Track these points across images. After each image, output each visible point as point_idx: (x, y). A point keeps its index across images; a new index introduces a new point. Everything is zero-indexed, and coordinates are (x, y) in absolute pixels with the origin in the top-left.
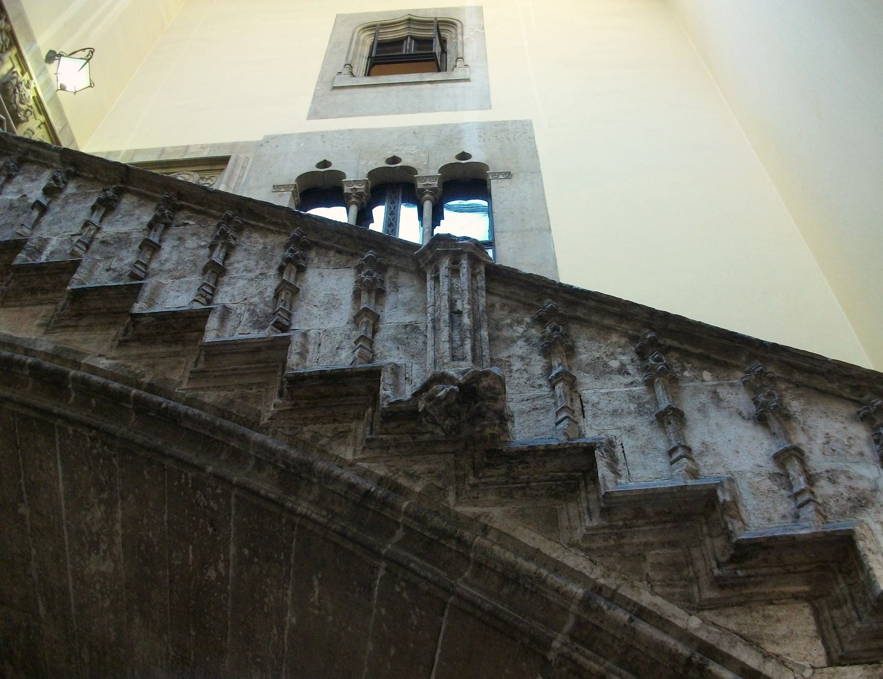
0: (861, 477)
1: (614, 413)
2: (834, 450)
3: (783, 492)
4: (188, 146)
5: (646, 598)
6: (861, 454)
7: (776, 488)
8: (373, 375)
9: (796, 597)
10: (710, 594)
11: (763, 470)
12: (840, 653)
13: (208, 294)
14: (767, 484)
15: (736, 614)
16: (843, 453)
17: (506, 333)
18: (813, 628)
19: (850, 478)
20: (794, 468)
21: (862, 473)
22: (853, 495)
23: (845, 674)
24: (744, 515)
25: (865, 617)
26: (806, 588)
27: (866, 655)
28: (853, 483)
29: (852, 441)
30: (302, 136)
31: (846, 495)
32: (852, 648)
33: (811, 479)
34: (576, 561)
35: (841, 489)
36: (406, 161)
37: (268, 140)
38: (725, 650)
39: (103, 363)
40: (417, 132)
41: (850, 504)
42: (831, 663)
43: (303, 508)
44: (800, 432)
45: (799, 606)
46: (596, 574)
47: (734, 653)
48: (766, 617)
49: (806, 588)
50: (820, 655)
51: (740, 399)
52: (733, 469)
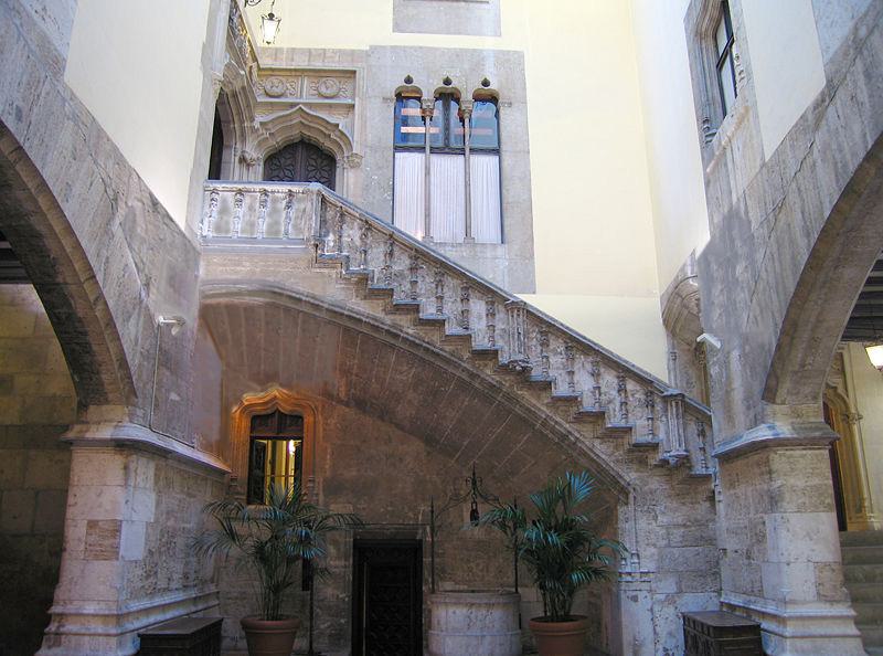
1: (558, 368)
4: (325, 50)
5: (558, 419)
8: (496, 352)
13: (440, 310)
17: (531, 335)
30: (394, 48)
34: (544, 409)
36: (455, 84)
37: (374, 49)
39: (410, 331)
40: (459, 54)
43: (477, 385)
46: (548, 412)
51: (589, 367)
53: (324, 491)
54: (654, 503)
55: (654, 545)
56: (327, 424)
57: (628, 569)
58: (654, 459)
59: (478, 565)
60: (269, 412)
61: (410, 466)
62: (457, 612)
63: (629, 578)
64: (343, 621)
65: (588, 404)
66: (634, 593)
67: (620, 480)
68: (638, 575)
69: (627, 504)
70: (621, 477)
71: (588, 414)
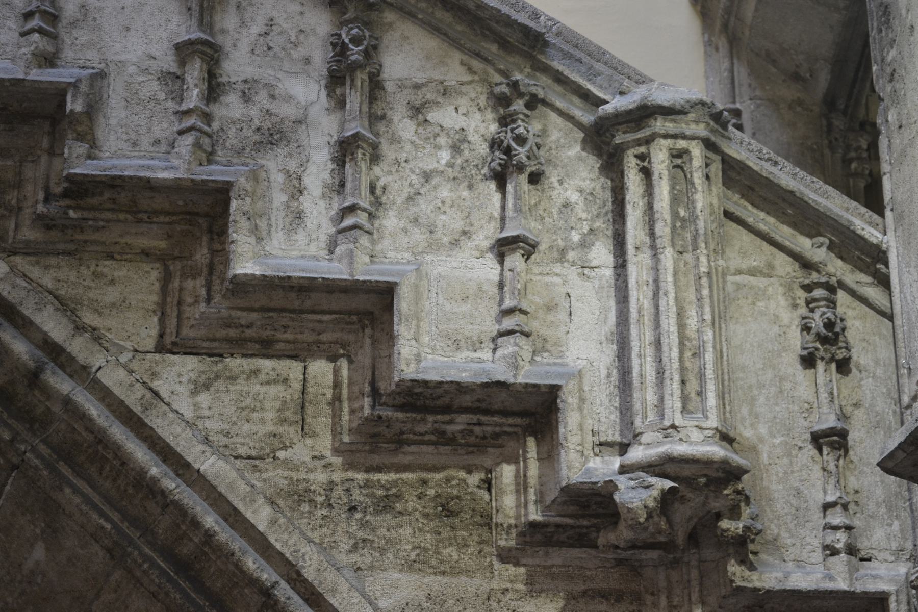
0: (289, 98)
2: (270, 48)
3: (170, 104)
6: (307, 61)
7: (162, 96)
9: (146, 254)
10: (29, 234)
11: (155, 66)
12: (174, 338)
14: (153, 87)
15: (58, 267)
16: (282, 54)
18: (154, 298)
19: (273, 97)
20: (194, 72)
21: (292, 93)
22: (267, 124)
23: (173, 364)
24: (100, 133)
25: (217, 298)
26: (163, 244)
27: (206, 344)
28: (274, 107)
29: (302, 37)
31: (257, 122)
32: (192, 334)
33: (214, 89)
35: (254, 112)
38: (27, 312)
41: (257, 138)
42: (160, 348)
44: (232, 10)
45: (146, 267)
47: (37, 319)
48: (96, 275)
49: (163, 244)
50: (150, 336)
52: (110, 57)
58: (515, 492)
65: (134, 141)
71: (127, 196)
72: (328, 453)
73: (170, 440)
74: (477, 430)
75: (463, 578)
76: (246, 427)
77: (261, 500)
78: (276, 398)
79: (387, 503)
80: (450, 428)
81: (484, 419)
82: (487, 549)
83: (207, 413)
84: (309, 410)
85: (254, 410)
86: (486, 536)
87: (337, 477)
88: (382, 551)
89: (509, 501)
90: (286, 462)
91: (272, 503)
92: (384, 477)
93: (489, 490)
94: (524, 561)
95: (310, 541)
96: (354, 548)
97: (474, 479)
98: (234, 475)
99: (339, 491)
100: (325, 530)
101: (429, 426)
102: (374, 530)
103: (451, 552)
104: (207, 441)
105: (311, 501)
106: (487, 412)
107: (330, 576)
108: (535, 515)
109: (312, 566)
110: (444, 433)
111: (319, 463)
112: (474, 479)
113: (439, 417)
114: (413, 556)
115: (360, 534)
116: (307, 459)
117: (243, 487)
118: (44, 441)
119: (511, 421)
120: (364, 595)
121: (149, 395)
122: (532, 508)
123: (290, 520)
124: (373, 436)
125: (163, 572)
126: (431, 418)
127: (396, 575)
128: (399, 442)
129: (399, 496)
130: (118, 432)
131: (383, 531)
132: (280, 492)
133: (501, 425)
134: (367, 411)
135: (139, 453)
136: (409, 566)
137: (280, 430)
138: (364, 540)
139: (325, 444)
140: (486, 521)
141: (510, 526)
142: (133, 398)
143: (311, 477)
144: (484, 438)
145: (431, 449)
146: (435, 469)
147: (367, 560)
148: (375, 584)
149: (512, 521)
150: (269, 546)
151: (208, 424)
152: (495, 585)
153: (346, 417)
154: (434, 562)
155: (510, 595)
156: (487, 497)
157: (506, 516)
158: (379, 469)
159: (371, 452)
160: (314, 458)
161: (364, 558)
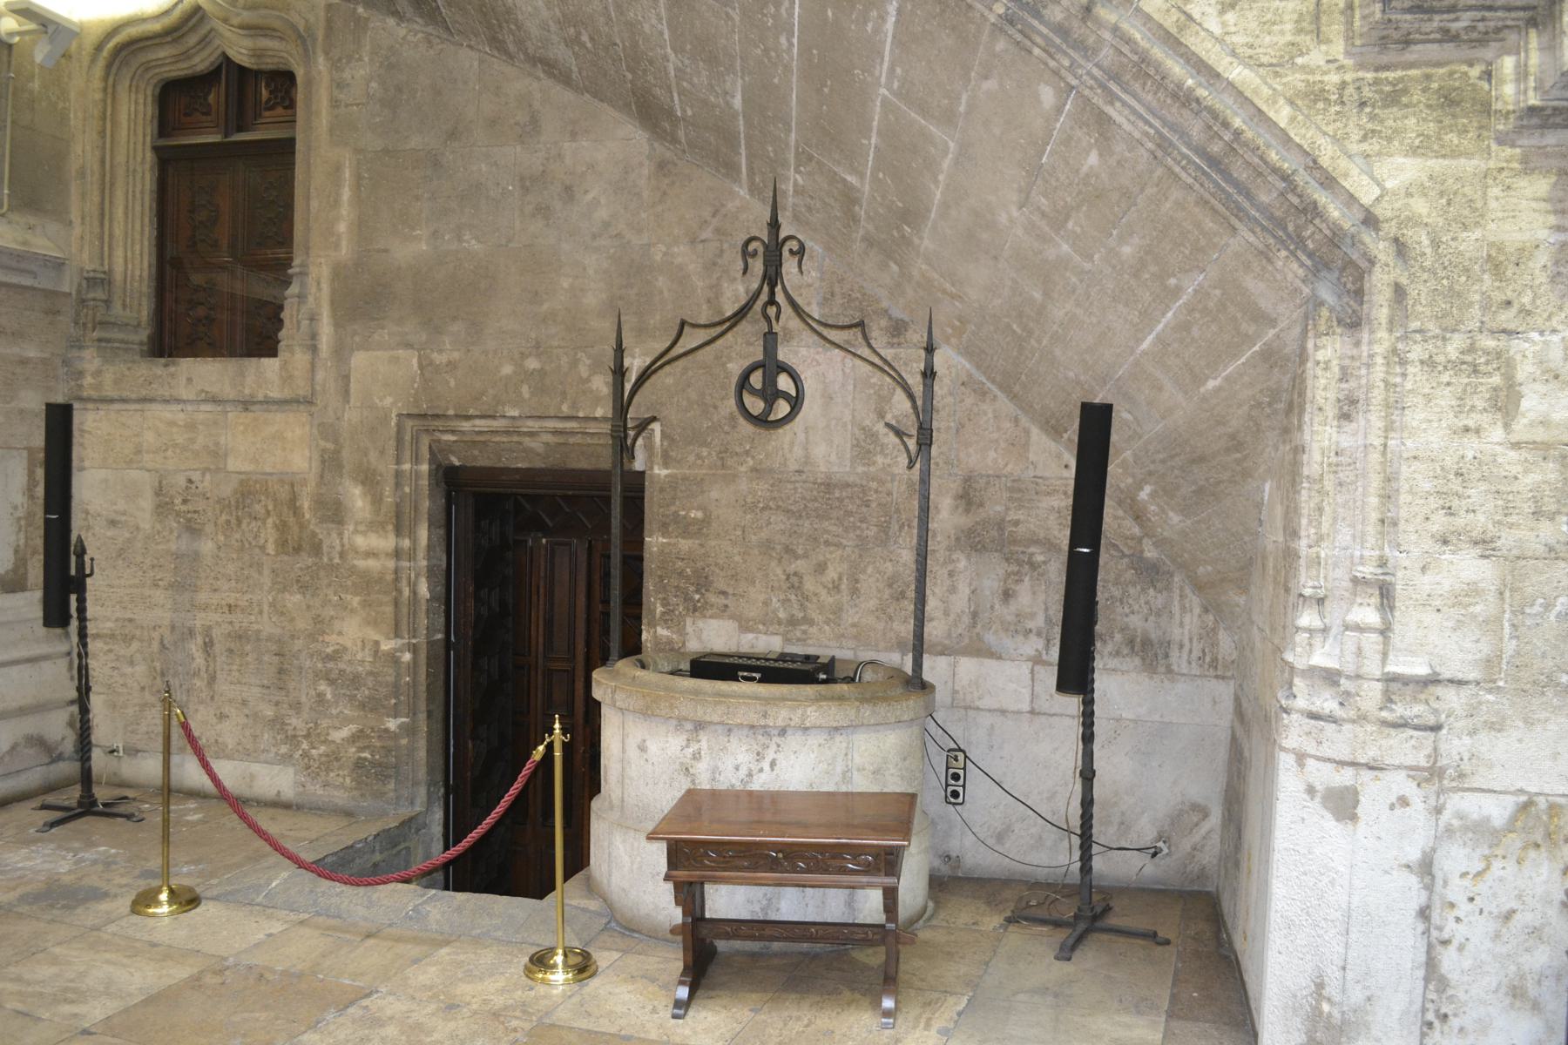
53: (332, 302)
54: (1506, 318)
55: (1485, 545)
56: (341, 85)
57: (1322, 658)
59: (821, 568)
60: (201, 63)
61: (602, 214)
62: (653, 747)
63: (1327, 703)
64: (392, 724)
66: (1346, 777)
67: (1322, 197)
68: (1371, 694)
69: (1353, 323)
70: (1329, 181)
72: (1341, 57)
73: (1203, 55)
74: (1481, 26)
75: (1463, 161)
76: (1268, 39)
77: (1282, 101)
78: (1294, 11)
79: (1394, 97)
80: (1455, 26)
81: (1487, 14)
82: (1485, 133)
83: (1233, 29)
84: (1324, 19)
85: (1274, 23)
86: (1485, 122)
87: (1348, 77)
88: (1389, 140)
89: (1509, 90)
90: (1303, 68)
91: (1291, 103)
92: (1391, 75)
93: (1489, 81)
94: (1519, 143)
95: (1325, 133)
96: (1364, 138)
97: (1475, 72)
98: (1258, 81)
99: (1350, 90)
100: (1338, 124)
101: (1435, 24)
102: (1382, 121)
103: (1452, 138)
104: (1234, 53)
105: (1326, 100)
106: (1490, 8)
107: (1343, 163)
108: (1533, 100)
109: (1327, 154)
110: (1448, 31)
111: (1332, 66)
112: (1475, 72)
113: (1445, 16)
114: (1417, 142)
115: (1370, 126)
116: (1322, 63)
117: (1266, 91)
118: (1097, 65)
119: (1514, 14)
120: (1372, 178)
121: (1183, 18)
122: (1531, 93)
123: (1307, 117)
124: (1383, 38)
125: (1199, 167)
126: (1437, 17)
127: (1401, 160)
128: (1407, 42)
129: (1405, 91)
130: (1158, 53)
131: (1391, 123)
132: (1298, 94)
133: (1503, 19)
134: (1378, 15)
135: (1176, 68)
136: (1414, 151)
137: (1298, 39)
138: (1373, 131)
139: (1338, 48)
140: (1485, 108)
141: (1508, 112)
142: (1170, 22)
143: (1326, 78)
144: (1487, 33)
145: (1436, 46)
146: (1439, 64)
147: (1377, 147)
148: (1382, 168)
149: (1511, 108)
150: (1290, 139)
151: (1235, 39)
152: (1492, 164)
153: (1357, 24)
154: (1436, 147)
155: (1505, 174)
156: (1486, 87)
157: (1506, 103)
158: (1387, 68)
159: (1380, 53)
160: (1328, 62)
161: (1373, 146)
